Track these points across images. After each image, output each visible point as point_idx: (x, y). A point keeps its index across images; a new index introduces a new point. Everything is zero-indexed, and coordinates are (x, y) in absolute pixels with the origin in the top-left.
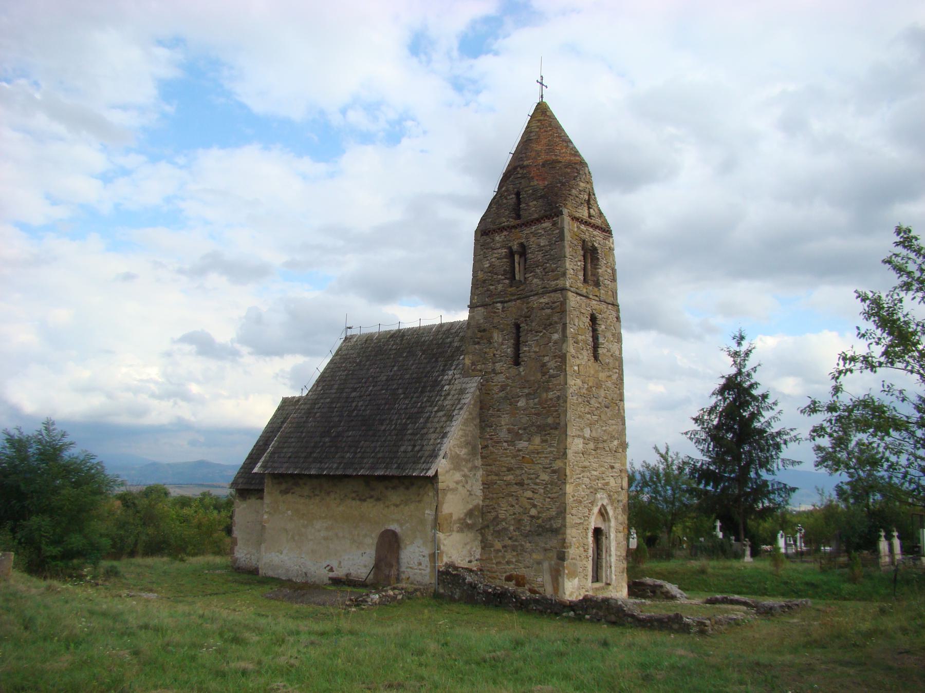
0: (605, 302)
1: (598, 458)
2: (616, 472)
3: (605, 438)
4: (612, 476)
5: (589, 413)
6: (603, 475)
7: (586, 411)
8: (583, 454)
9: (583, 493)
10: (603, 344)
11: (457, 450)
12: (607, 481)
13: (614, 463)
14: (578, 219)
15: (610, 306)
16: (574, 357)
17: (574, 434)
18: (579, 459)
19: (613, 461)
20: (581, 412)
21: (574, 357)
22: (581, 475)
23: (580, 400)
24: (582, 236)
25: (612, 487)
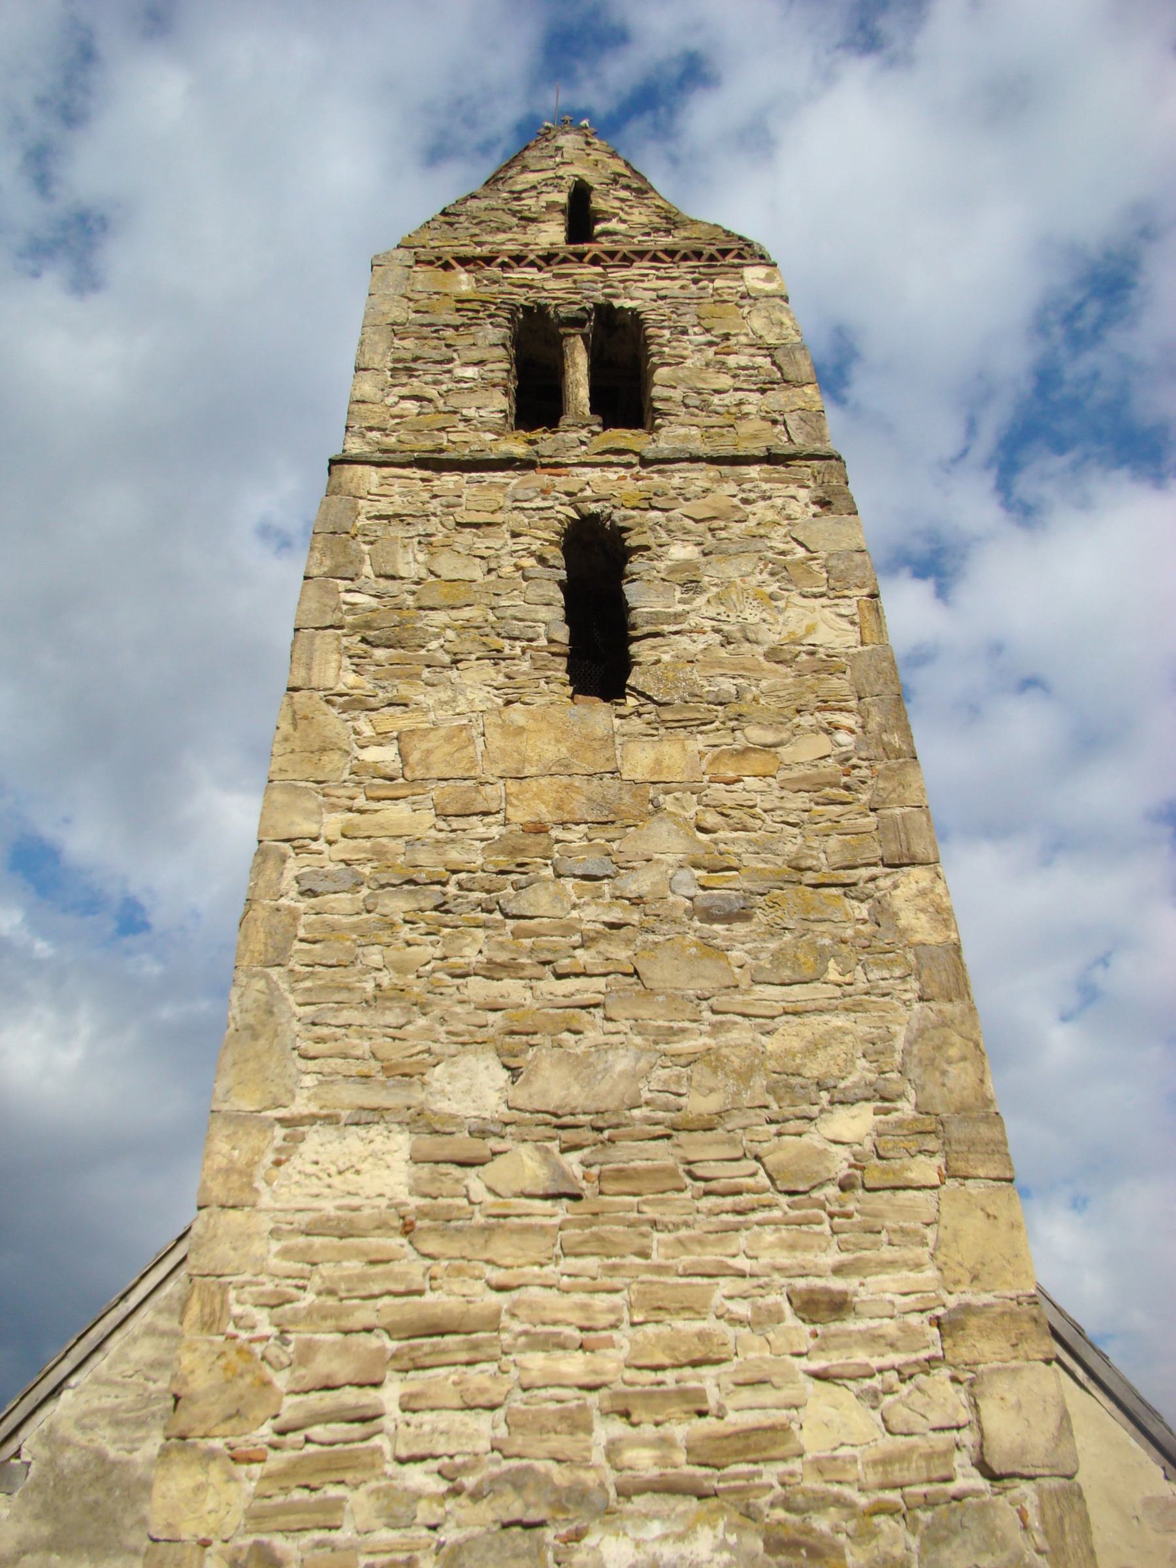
0: (694, 459)
1: (603, 1246)
2: (873, 1339)
3: (699, 1104)
4: (820, 1376)
5: (493, 970)
6: (707, 1379)
7: (471, 953)
8: (408, 1229)
9: (385, 1535)
10: (678, 617)
11: (106, 1441)
12: (736, 1420)
13: (838, 1270)
14: (489, 260)
15: (753, 471)
16: (355, 704)
17: (301, 1106)
18: (354, 1266)
19: (833, 1257)
20: (400, 968)
21: (355, 704)
22: (389, 1395)
23: (397, 905)
24: (521, 298)
25: (820, 1466)
